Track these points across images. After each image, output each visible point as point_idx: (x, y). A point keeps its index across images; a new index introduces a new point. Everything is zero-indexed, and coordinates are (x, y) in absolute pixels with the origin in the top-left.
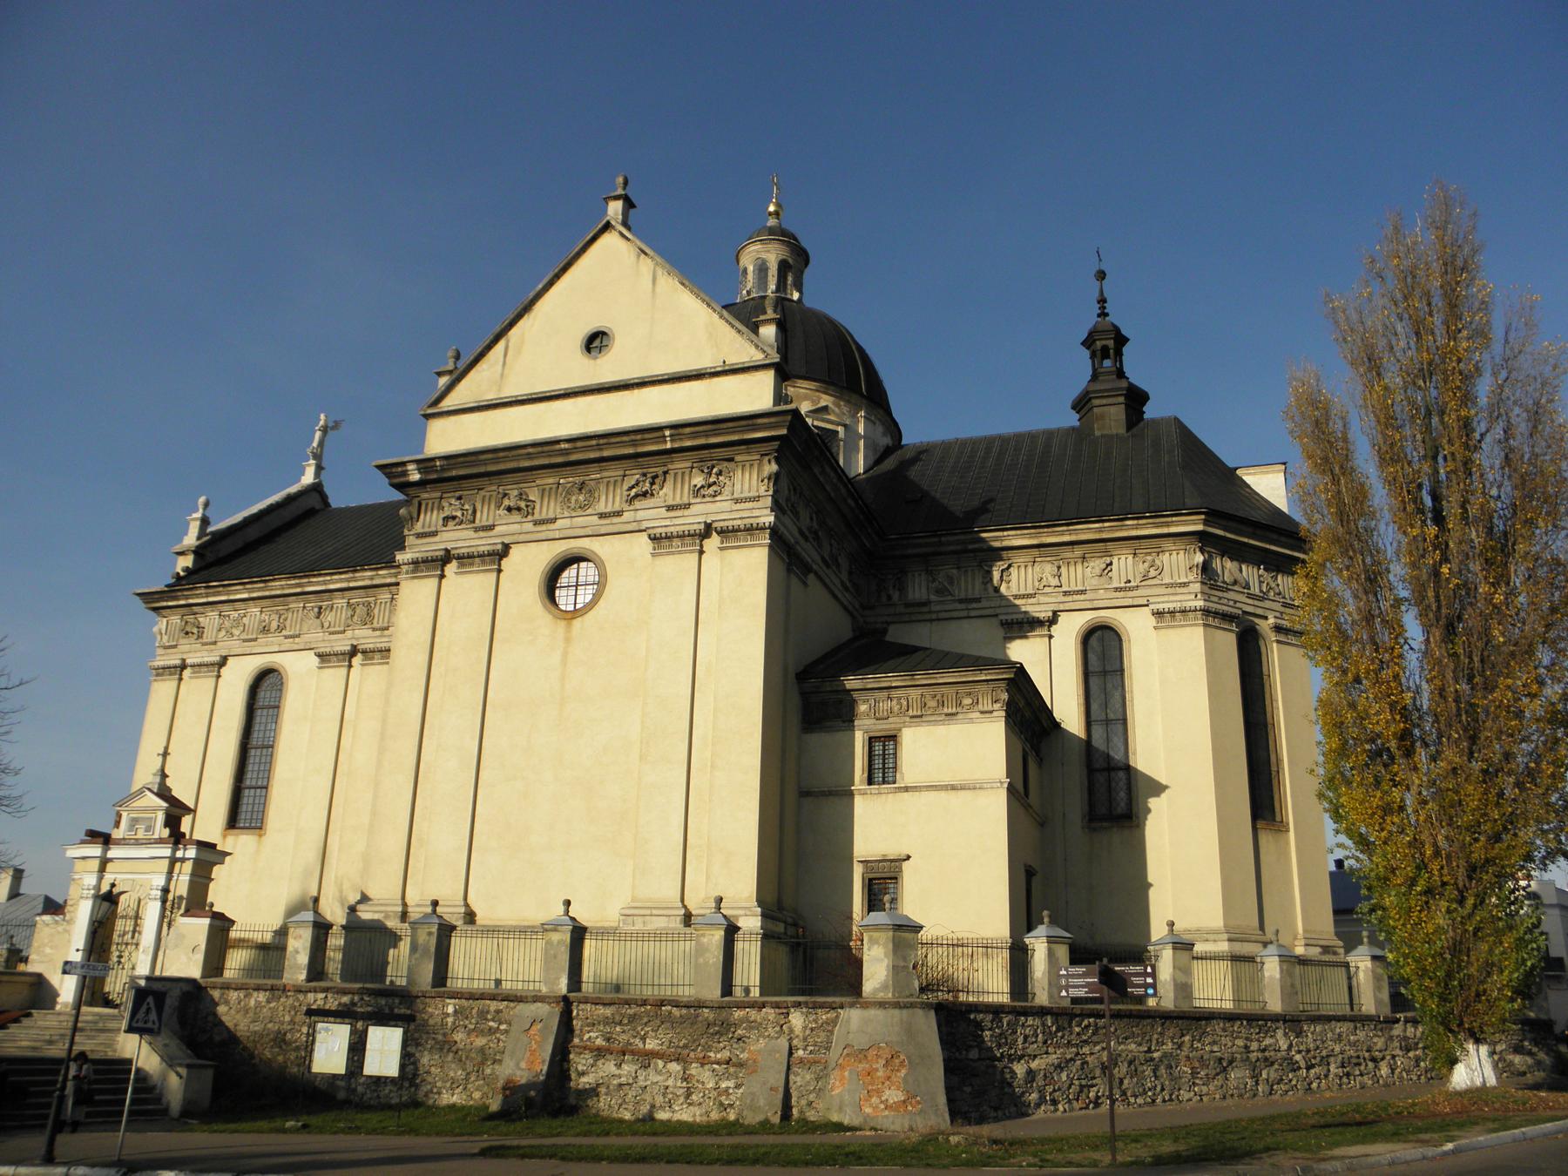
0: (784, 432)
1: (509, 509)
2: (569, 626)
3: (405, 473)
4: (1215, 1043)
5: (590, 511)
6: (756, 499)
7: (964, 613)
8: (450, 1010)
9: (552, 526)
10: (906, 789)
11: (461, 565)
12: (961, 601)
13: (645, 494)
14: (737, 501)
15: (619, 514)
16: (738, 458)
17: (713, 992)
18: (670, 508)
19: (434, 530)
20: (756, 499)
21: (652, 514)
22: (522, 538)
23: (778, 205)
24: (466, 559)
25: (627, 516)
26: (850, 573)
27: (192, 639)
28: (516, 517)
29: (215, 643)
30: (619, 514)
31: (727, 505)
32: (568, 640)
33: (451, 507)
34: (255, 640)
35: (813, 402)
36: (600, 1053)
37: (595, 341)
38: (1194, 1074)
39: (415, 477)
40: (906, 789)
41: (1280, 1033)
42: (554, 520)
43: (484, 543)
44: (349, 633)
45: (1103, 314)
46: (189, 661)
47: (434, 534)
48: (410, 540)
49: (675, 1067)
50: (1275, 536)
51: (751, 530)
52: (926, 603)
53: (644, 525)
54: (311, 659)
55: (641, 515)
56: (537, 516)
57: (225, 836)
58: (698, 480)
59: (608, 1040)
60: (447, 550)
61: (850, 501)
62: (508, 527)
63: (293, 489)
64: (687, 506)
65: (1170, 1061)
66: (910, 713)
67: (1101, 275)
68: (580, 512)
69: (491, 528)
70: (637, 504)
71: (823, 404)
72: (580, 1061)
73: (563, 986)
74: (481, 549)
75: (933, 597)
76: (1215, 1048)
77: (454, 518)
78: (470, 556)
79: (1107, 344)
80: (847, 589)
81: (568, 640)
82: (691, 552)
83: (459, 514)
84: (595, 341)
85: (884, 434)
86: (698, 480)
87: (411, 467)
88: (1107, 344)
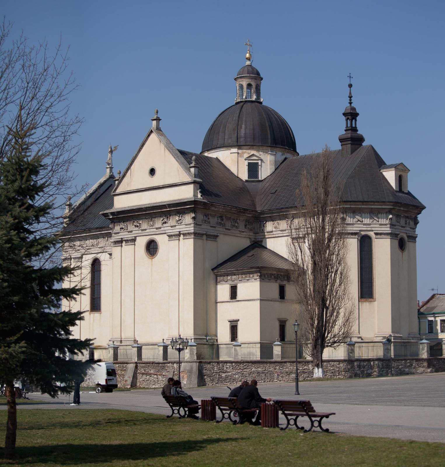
0: (193, 206)
1: (135, 226)
2: (152, 261)
3: (108, 216)
4: (287, 368)
5: (154, 227)
6: (190, 224)
7: (282, 235)
8: (117, 366)
9: (146, 231)
10: (238, 301)
11: (126, 243)
12: (282, 231)
13: (165, 223)
14: (186, 225)
15: (160, 228)
16: (186, 212)
17: (161, 360)
18: (172, 227)
19: (119, 231)
20: (190, 224)
21: (167, 228)
22: (139, 235)
23: (250, 55)
24: (127, 241)
25: (162, 229)
26: (246, 226)
28: (137, 229)
30: (160, 228)
31: (184, 226)
32: (152, 265)
33: (122, 225)
35: (249, 153)
36: (143, 374)
37: (152, 172)
38: (278, 375)
39: (111, 217)
40: (238, 301)
41: (310, 366)
42: (146, 230)
43: (129, 236)
45: (351, 103)
46: (72, 257)
47: (118, 233)
48: (113, 235)
49: (155, 376)
50: (373, 203)
52: (272, 232)
55: (165, 228)
56: (142, 228)
57: (90, 314)
58: (177, 218)
59: (145, 371)
60: (122, 238)
61: (233, 209)
62: (136, 232)
63: (102, 180)
64: (175, 226)
65: (271, 373)
66: (239, 279)
67: (350, 86)
68: (151, 227)
69: (131, 232)
70: (164, 225)
71: (252, 153)
72: (139, 376)
73: (136, 360)
74: (130, 238)
75: (274, 230)
76: (287, 369)
77: (123, 228)
78: (127, 240)
79: (352, 115)
80: (243, 232)
81: (152, 265)
82: (177, 240)
83: (124, 227)
84: (152, 172)
85: (282, 155)
86: (177, 218)
87: (109, 214)
88: (352, 115)
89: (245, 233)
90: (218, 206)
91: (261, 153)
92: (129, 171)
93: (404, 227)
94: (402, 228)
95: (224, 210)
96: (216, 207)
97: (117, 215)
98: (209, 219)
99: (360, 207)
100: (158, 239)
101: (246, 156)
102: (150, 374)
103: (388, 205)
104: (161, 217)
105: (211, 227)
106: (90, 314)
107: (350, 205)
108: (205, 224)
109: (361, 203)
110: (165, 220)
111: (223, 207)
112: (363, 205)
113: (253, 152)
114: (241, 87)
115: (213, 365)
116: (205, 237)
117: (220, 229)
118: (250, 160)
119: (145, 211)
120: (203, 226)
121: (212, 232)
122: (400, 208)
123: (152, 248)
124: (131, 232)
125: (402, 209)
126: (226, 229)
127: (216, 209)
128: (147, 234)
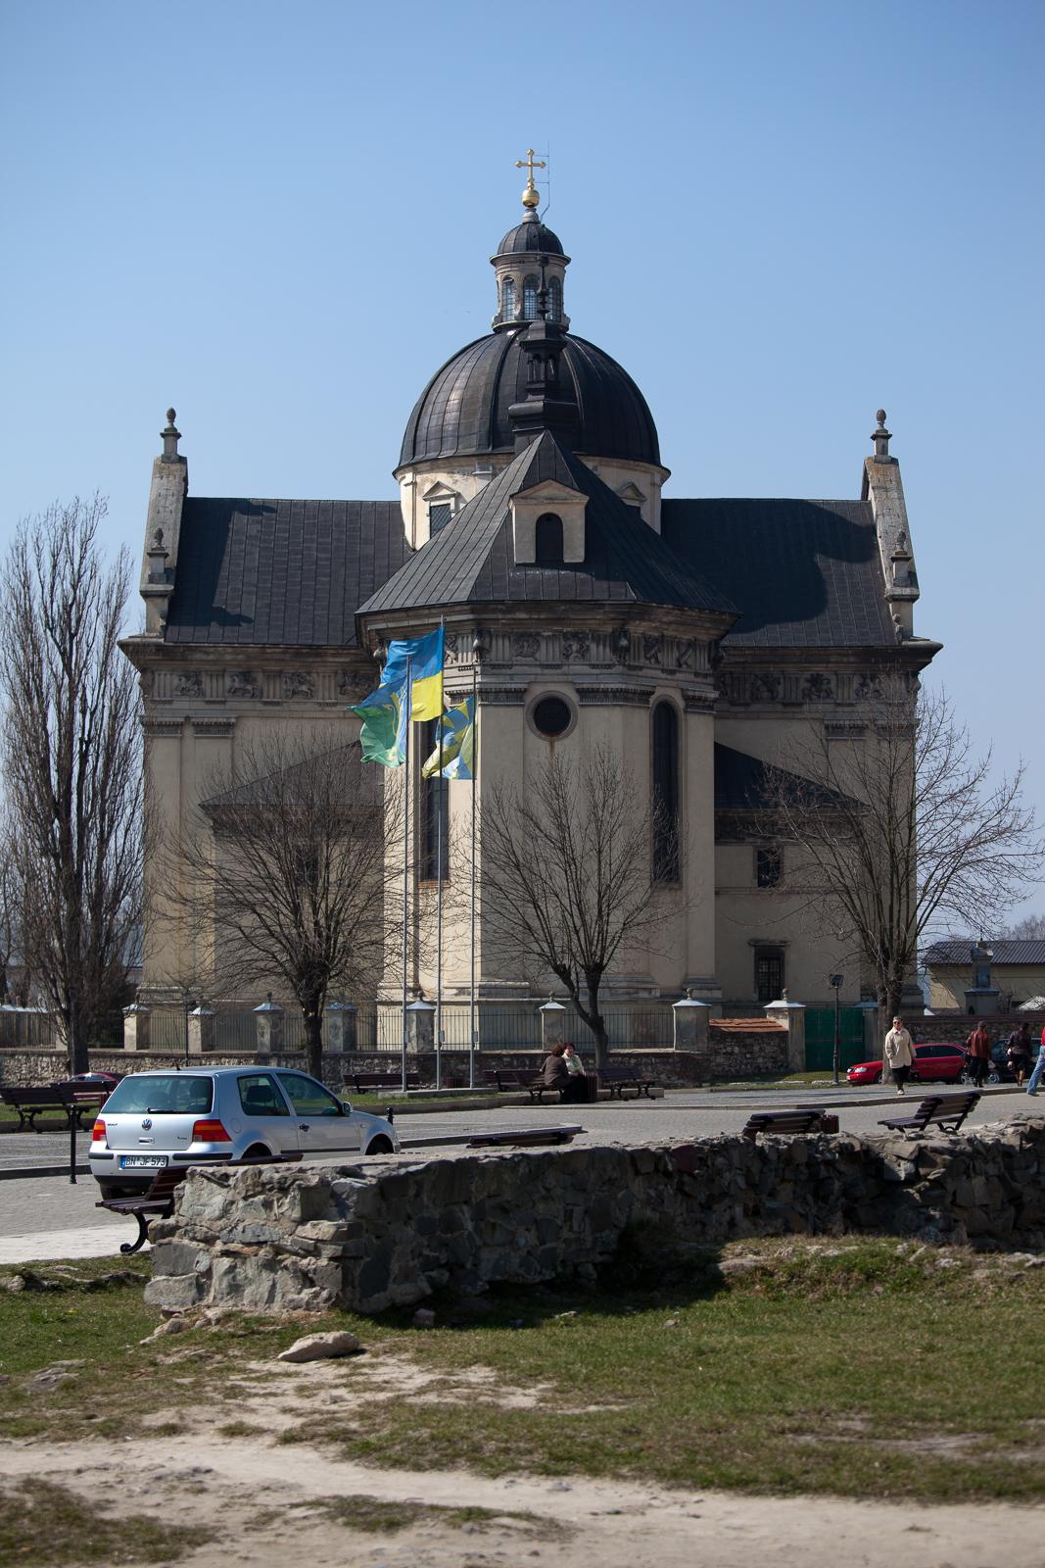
50: (427, 611)
89: (338, 708)
90: (212, 650)
91: (457, 477)
93: (558, 666)
94: (546, 671)
95: (241, 657)
96: (206, 653)
98: (198, 683)
99: (406, 624)
101: (428, 487)
103: (460, 613)
105: (207, 702)
107: (385, 621)
108: (183, 698)
109: (404, 614)
111: (229, 650)
112: (409, 618)
113: (442, 477)
115: (19, 1061)
116: (189, 732)
117: (246, 705)
118: (432, 500)
120: (176, 705)
121: (216, 715)
122: (509, 616)
125: (523, 616)
126: (265, 703)
127: (211, 657)
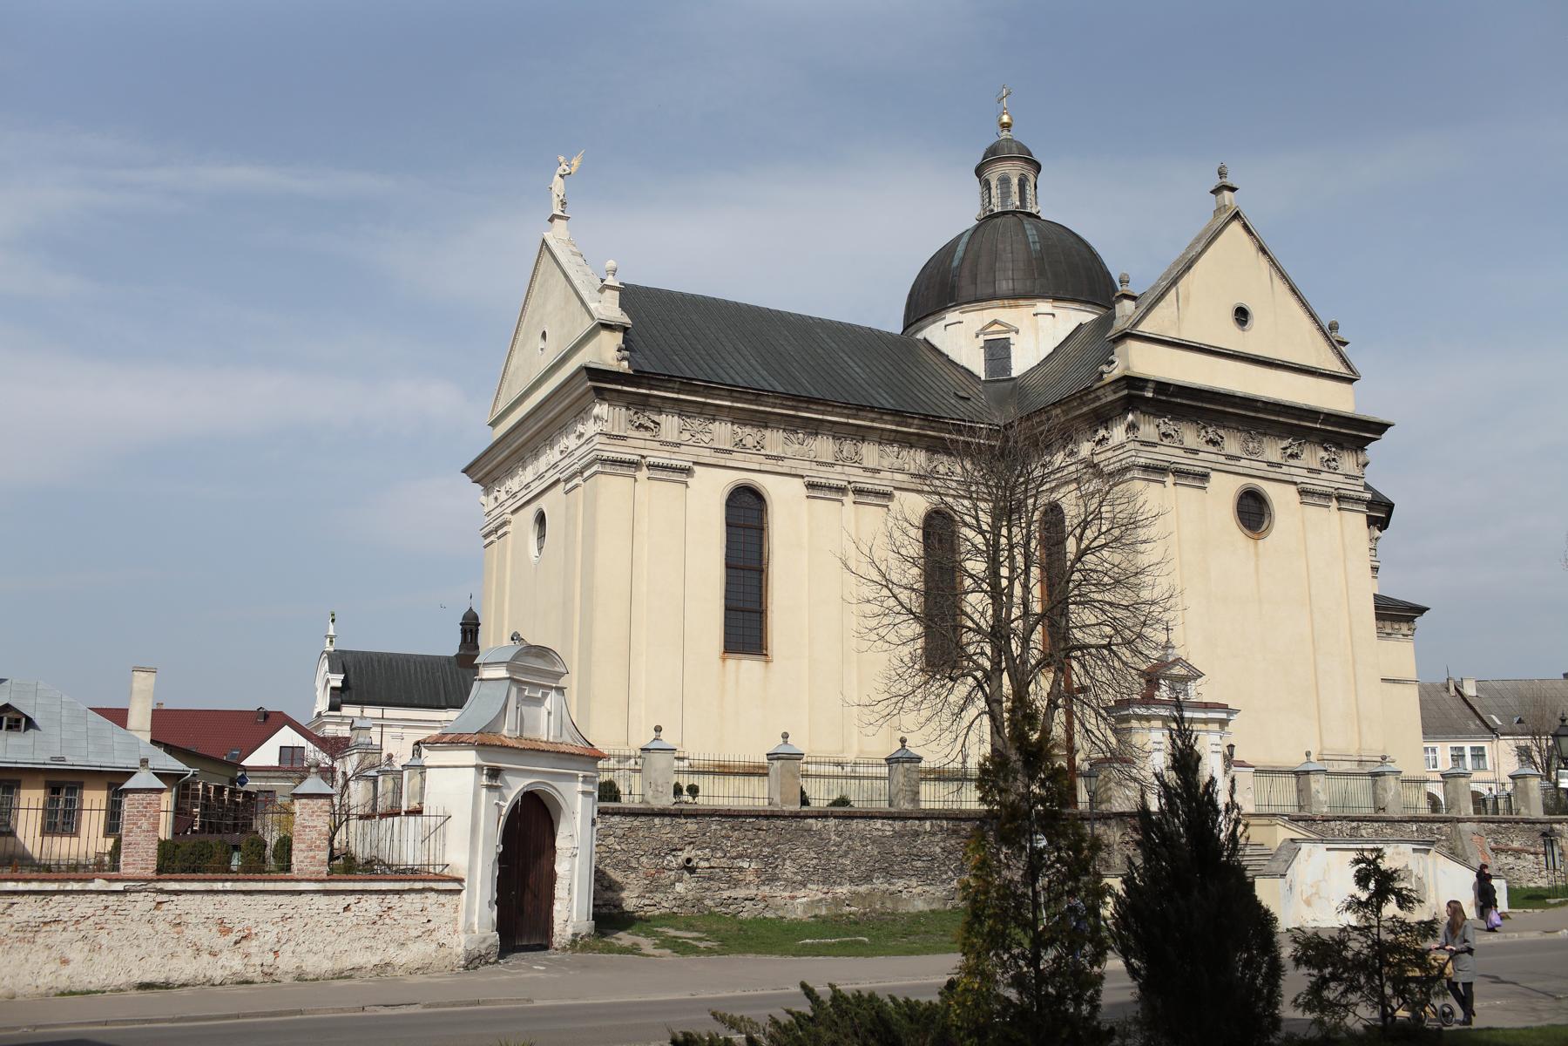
18: (1311, 470)
24: (1179, 473)
27: (647, 435)
28: (1211, 448)
29: (678, 445)
30: (1280, 465)
31: (1341, 478)
33: (1168, 426)
34: (730, 452)
42: (1238, 458)
44: (839, 469)
47: (1154, 445)
51: (1358, 500)
53: (1298, 480)
54: (798, 484)
55: (1293, 470)
57: (724, 660)
62: (1207, 457)
70: (1292, 462)
81: (1257, 554)
92: (1173, 291)
97: (1173, 395)
100: (1270, 490)
102: (1517, 853)
104: (1282, 438)
106: (724, 660)
110: (1295, 450)
114: (1005, 181)
119: (1257, 410)
123: (1253, 511)
124: (1196, 452)
128: (1241, 470)
